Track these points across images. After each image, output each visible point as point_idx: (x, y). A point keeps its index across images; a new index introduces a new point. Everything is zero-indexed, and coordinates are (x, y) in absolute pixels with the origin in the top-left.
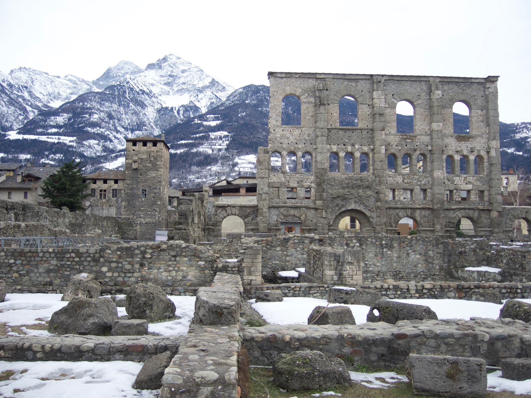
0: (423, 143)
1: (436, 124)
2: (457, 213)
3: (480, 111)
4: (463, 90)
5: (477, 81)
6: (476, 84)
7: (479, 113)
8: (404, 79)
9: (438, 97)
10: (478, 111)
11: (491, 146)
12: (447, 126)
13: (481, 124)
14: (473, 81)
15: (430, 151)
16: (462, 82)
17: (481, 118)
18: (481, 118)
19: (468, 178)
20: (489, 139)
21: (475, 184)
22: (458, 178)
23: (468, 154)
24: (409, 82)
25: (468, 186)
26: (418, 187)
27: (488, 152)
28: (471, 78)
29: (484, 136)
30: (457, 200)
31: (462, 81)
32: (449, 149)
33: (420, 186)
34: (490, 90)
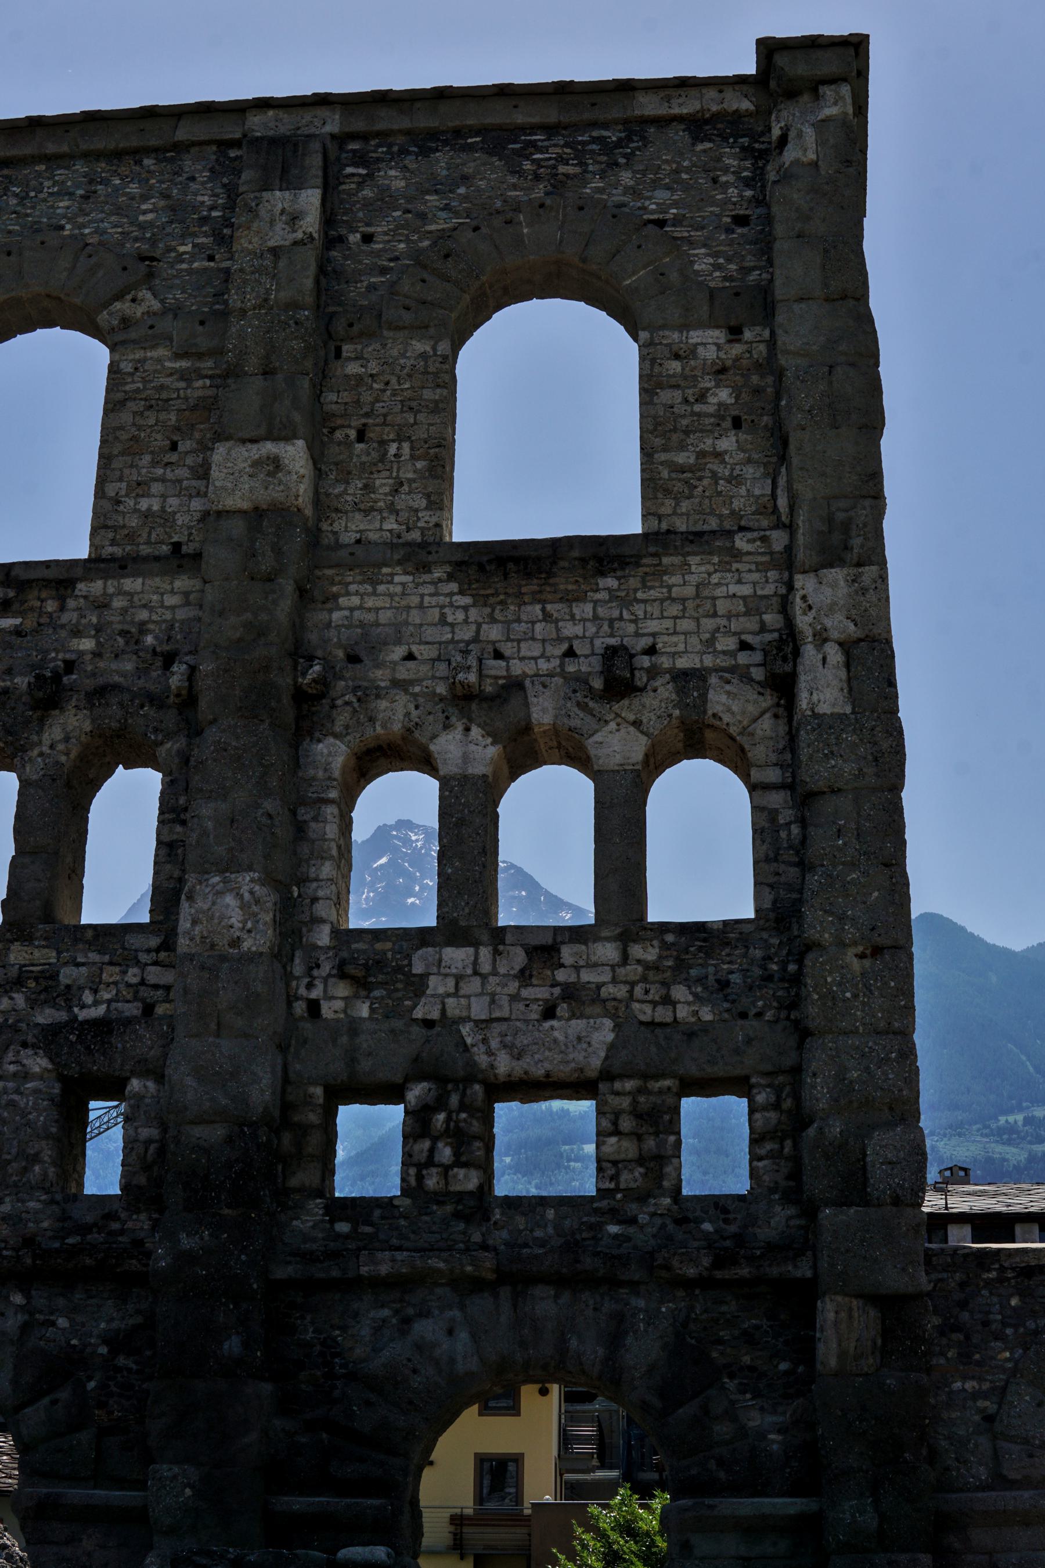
0: (133, 636)
1: (245, 455)
2: (425, 1329)
3: (718, 335)
4: (558, 185)
5: (686, 106)
6: (679, 135)
7: (709, 354)
8: (27, 150)
9: (280, 236)
10: (695, 336)
11: (803, 621)
12: (383, 484)
13: (727, 443)
14: (649, 106)
15: (189, 700)
16: (551, 130)
17: (724, 395)
18: (724, 395)
19: (567, 954)
20: (787, 563)
21: (644, 1012)
22: (457, 956)
23: (578, 720)
24: (80, 167)
25: (559, 1029)
26: (38, 1063)
27: (783, 686)
28: (626, 87)
29: (741, 543)
30: (432, 1182)
31: (551, 115)
32: (381, 676)
33: (49, 1039)
34: (790, 154)
